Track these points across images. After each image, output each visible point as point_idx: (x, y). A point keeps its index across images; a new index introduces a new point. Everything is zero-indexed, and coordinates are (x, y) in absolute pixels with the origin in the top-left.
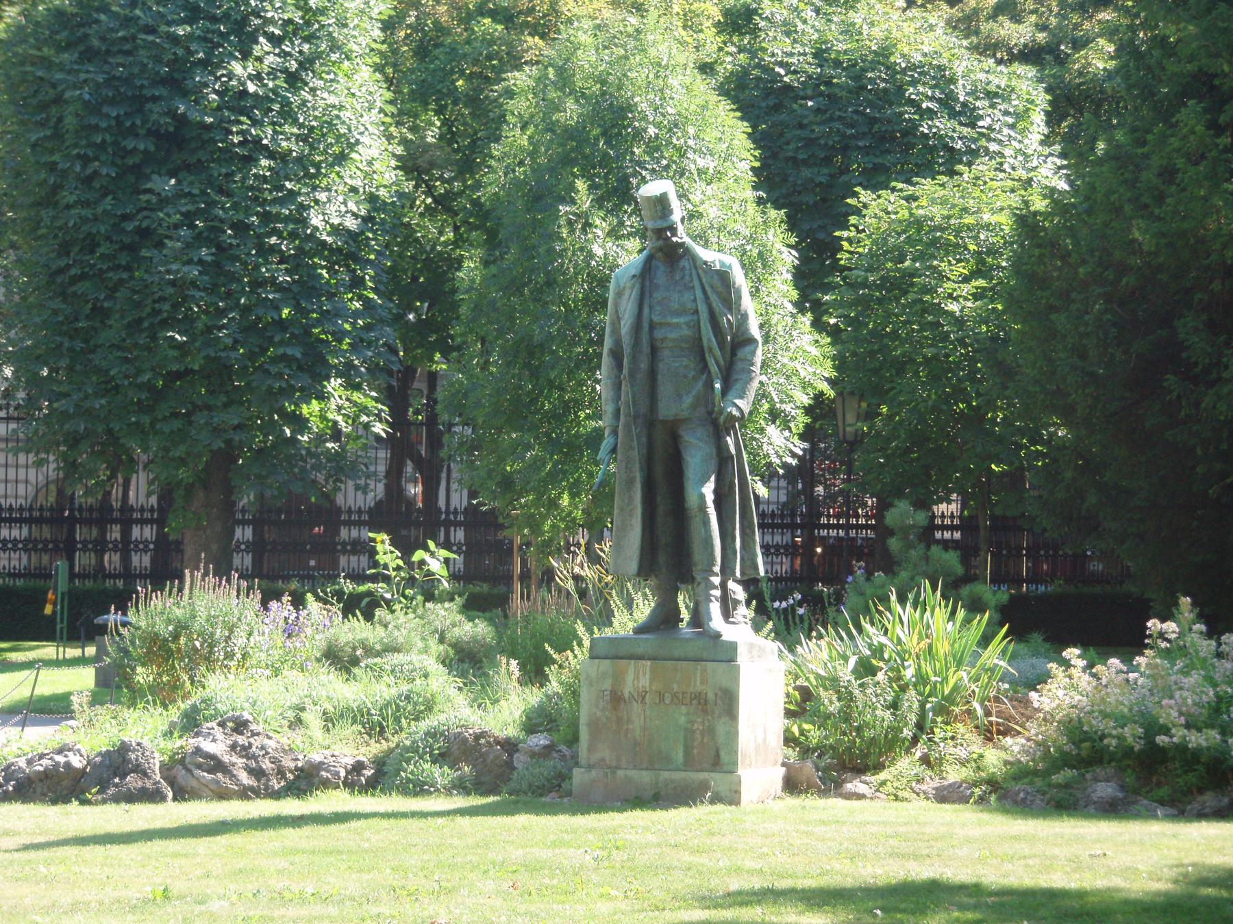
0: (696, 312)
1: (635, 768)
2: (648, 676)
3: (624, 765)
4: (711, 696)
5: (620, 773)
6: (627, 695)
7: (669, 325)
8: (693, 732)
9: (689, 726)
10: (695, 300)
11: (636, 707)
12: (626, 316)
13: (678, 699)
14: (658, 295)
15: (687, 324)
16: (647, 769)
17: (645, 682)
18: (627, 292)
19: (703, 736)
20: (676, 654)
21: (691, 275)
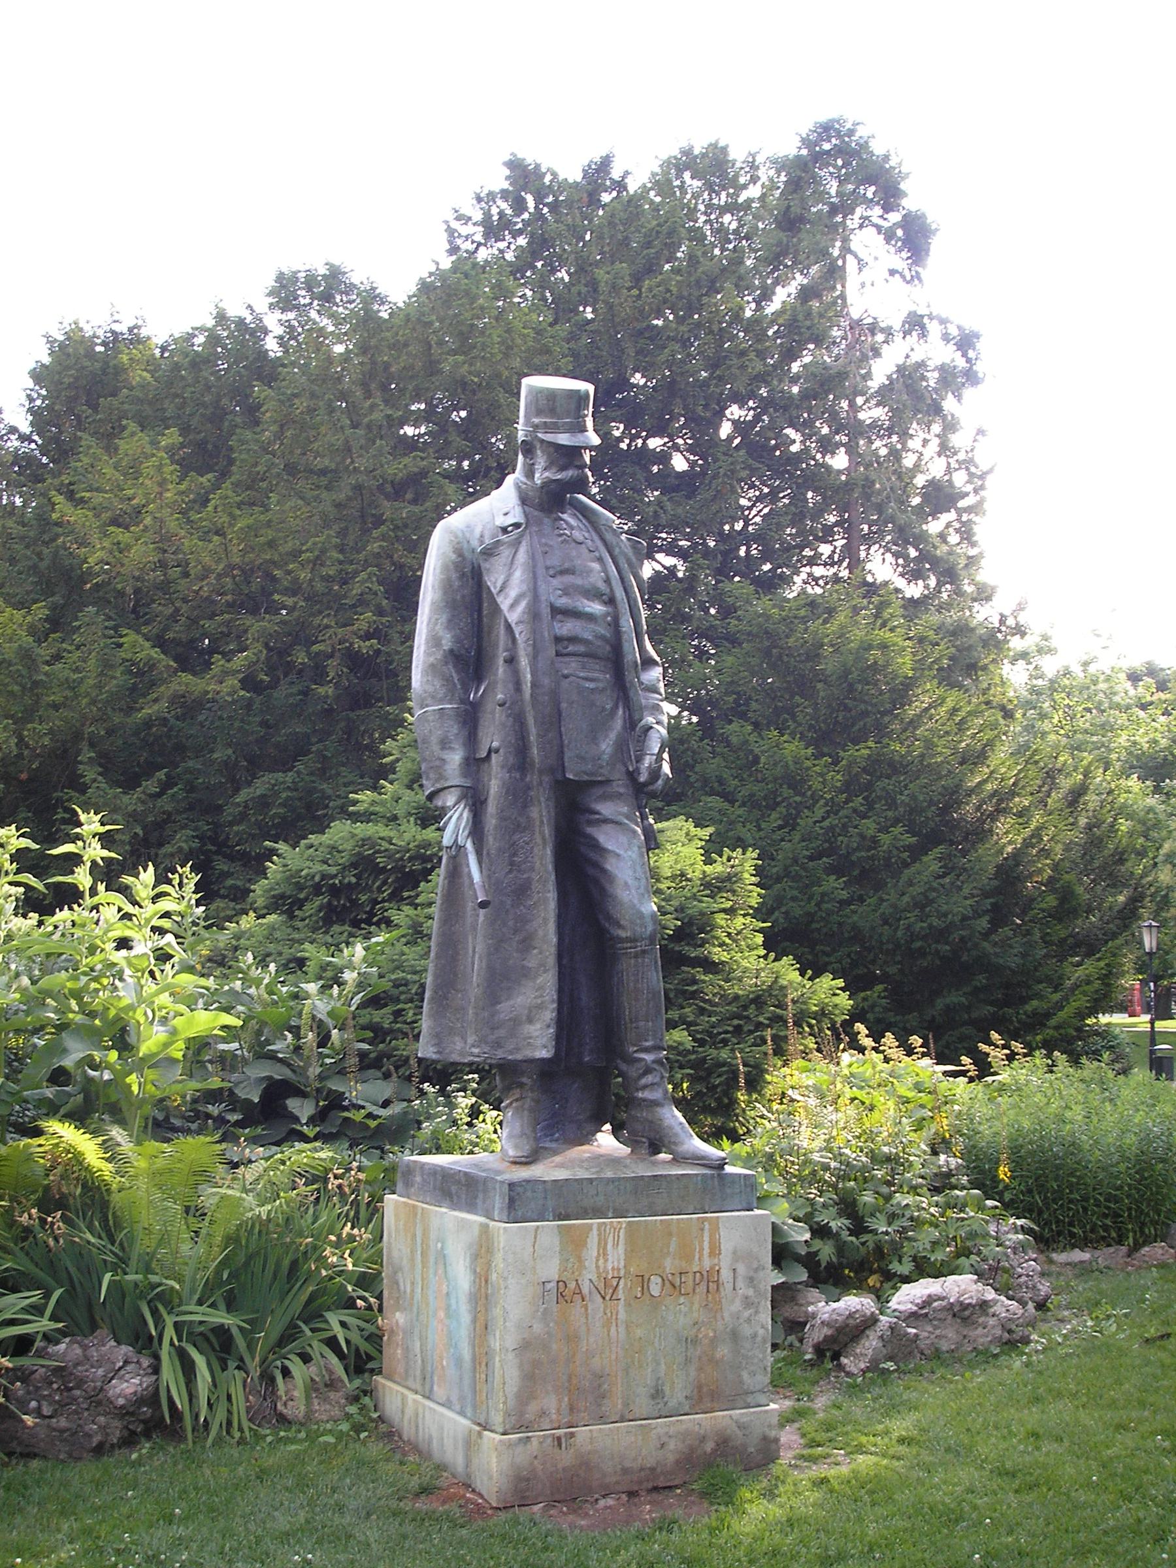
0: (611, 601)
10: (607, 581)
13: (673, 1286)
17: (616, 1257)
18: (506, 553)
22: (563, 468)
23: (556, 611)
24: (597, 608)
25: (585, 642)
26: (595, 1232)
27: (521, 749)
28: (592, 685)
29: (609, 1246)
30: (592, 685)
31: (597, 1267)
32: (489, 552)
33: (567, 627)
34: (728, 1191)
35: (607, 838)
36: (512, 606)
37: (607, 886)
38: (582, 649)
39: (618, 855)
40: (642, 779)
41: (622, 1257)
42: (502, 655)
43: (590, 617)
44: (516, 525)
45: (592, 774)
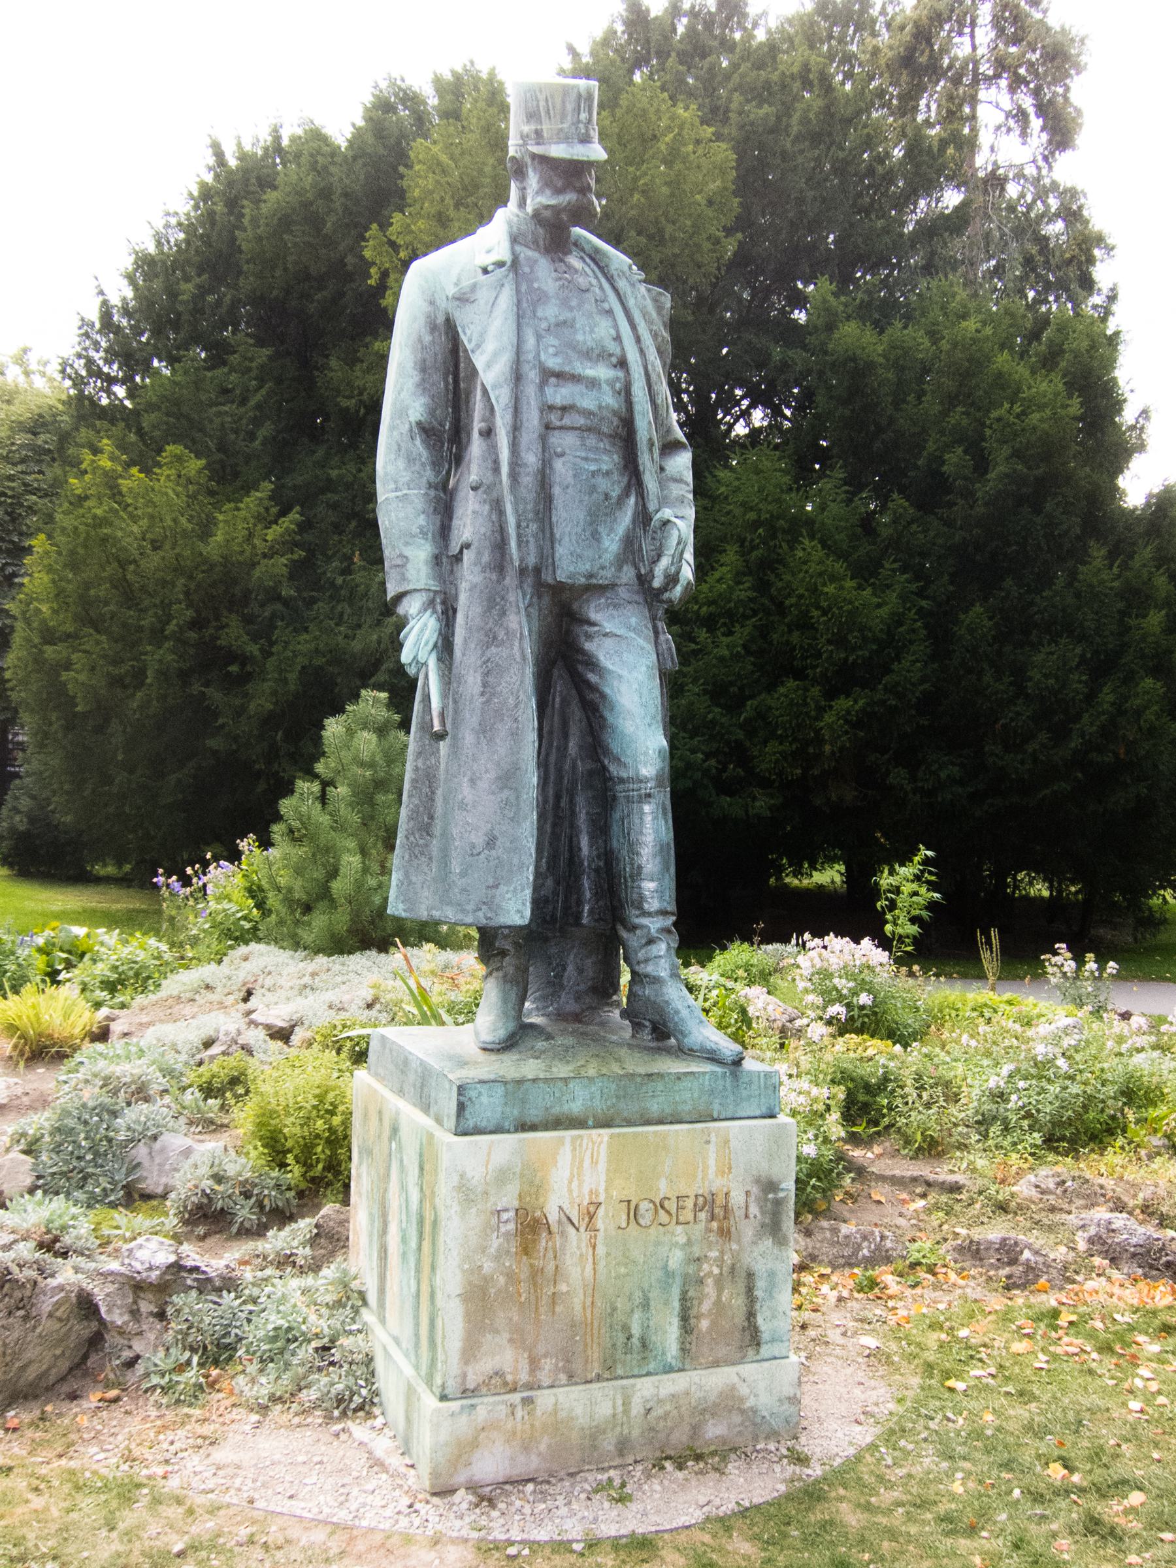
0: (622, 363)
1: (572, 1379)
2: (602, 1166)
3: (544, 1378)
4: (737, 1199)
5: (545, 1399)
6: (553, 1217)
7: (575, 378)
8: (701, 1282)
9: (691, 1269)
10: (618, 338)
11: (576, 1241)
12: (490, 346)
14: (550, 312)
16: (599, 1378)
18: (484, 296)
19: (720, 1291)
20: (655, 1108)
21: (601, 288)
22: (558, 191)
23: (547, 375)
24: (603, 372)
25: (588, 413)
26: (568, 1147)
27: (500, 545)
28: (593, 468)
31: (570, 1191)
32: (463, 299)
33: (559, 394)
34: (745, 1093)
35: (603, 651)
36: (489, 365)
37: (607, 714)
38: (581, 421)
39: (620, 677)
40: (656, 584)
41: (603, 1178)
42: (477, 425)
43: (593, 383)
44: (500, 264)
45: (591, 576)
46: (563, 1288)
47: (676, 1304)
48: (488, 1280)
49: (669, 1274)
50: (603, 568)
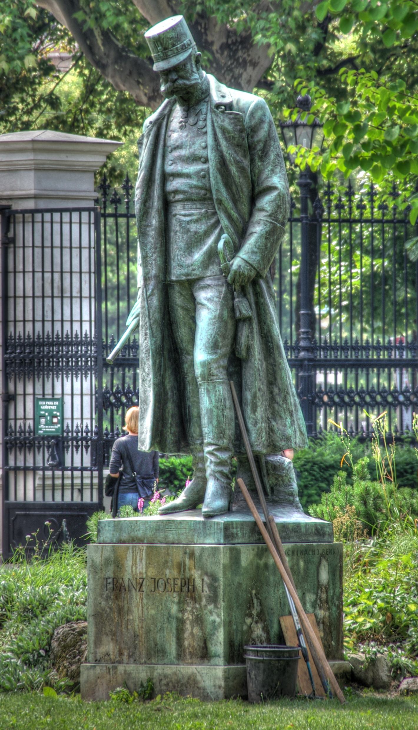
0: (206, 161)
2: (144, 562)
6: (126, 583)
9: (180, 615)
11: (136, 596)
15: (197, 173)
25: (184, 192)
28: (188, 219)
29: (138, 560)
30: (188, 219)
34: (208, 532)
43: (188, 176)
45: (187, 275)
46: (131, 618)
47: (174, 631)
48: (103, 610)
49: (170, 616)
50: (194, 270)
